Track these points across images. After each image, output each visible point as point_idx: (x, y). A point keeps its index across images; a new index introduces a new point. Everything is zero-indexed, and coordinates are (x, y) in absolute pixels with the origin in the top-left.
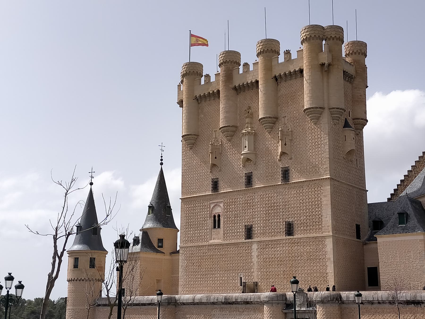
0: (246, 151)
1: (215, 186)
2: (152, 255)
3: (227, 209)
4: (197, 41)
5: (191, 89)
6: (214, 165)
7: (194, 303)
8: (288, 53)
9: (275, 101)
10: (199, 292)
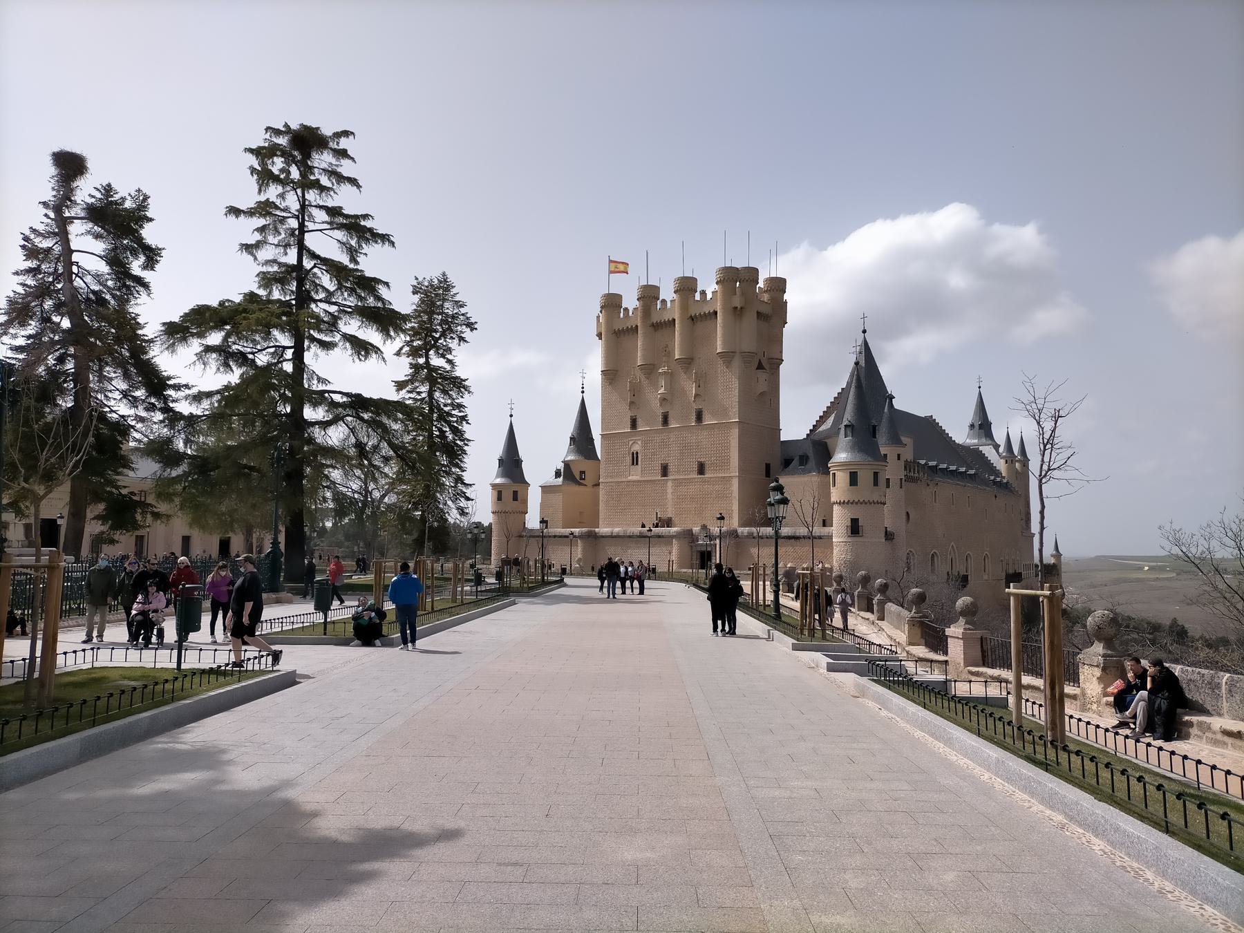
0: (662, 391)
1: (634, 424)
2: (575, 488)
3: (644, 446)
4: (617, 267)
5: (609, 321)
6: (632, 403)
7: (612, 537)
8: (703, 293)
9: (691, 342)
10: (618, 525)
